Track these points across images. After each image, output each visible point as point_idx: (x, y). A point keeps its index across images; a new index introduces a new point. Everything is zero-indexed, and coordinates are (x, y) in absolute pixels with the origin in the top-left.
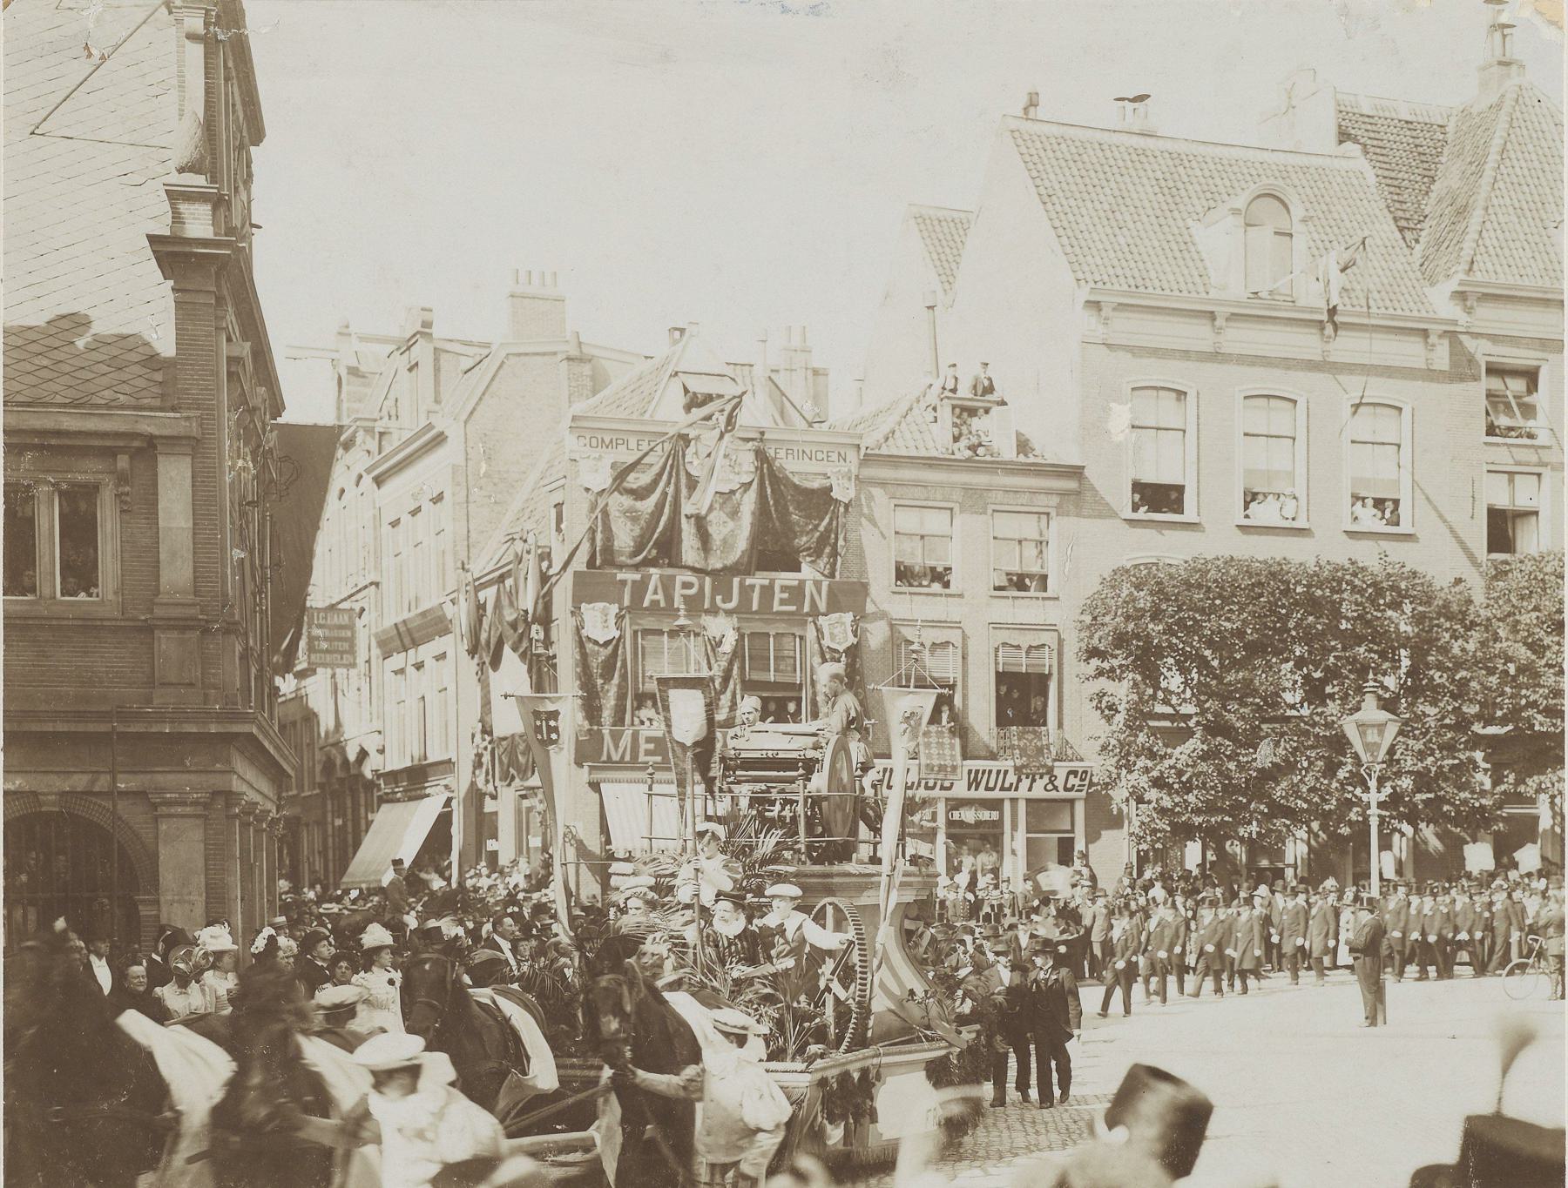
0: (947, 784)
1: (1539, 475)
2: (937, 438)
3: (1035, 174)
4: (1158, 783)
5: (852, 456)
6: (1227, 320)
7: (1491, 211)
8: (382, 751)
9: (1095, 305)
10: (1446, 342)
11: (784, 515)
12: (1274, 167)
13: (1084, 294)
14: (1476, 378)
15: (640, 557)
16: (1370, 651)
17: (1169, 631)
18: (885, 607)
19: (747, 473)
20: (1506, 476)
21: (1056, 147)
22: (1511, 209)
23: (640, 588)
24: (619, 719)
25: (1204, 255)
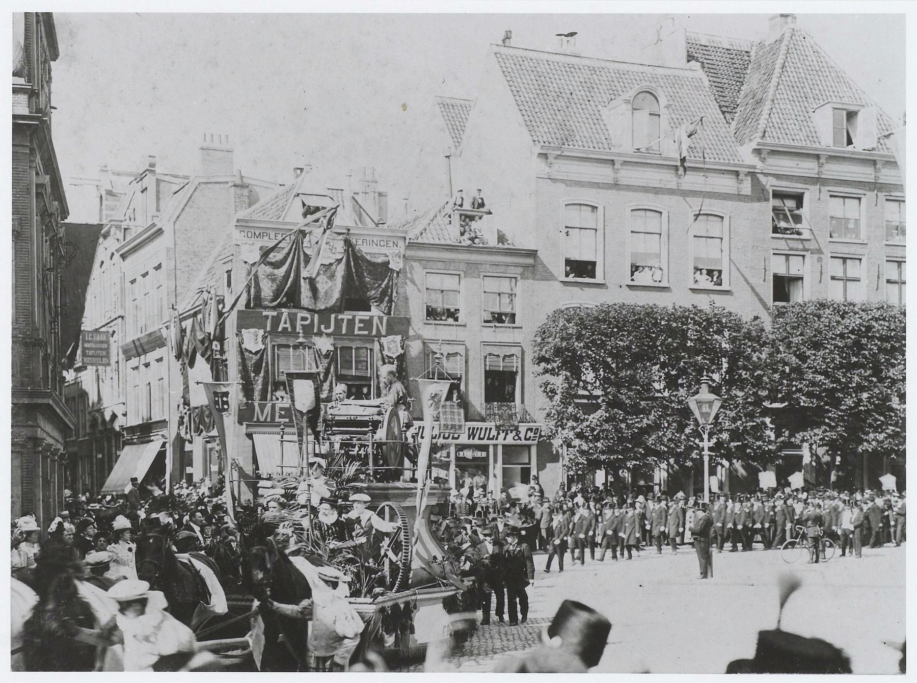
0: (456, 436)
1: (803, 256)
2: (452, 233)
3: (509, 79)
4: (580, 436)
5: (401, 243)
6: (622, 164)
7: (776, 102)
8: (125, 415)
9: (544, 156)
10: (749, 178)
11: (361, 277)
12: (649, 75)
13: (538, 150)
14: (767, 200)
15: (275, 303)
16: (704, 358)
17: (587, 347)
18: (420, 332)
19: (339, 253)
20: (784, 257)
21: (521, 63)
22: (788, 102)
23: (276, 320)
24: (264, 397)
25: (608, 128)
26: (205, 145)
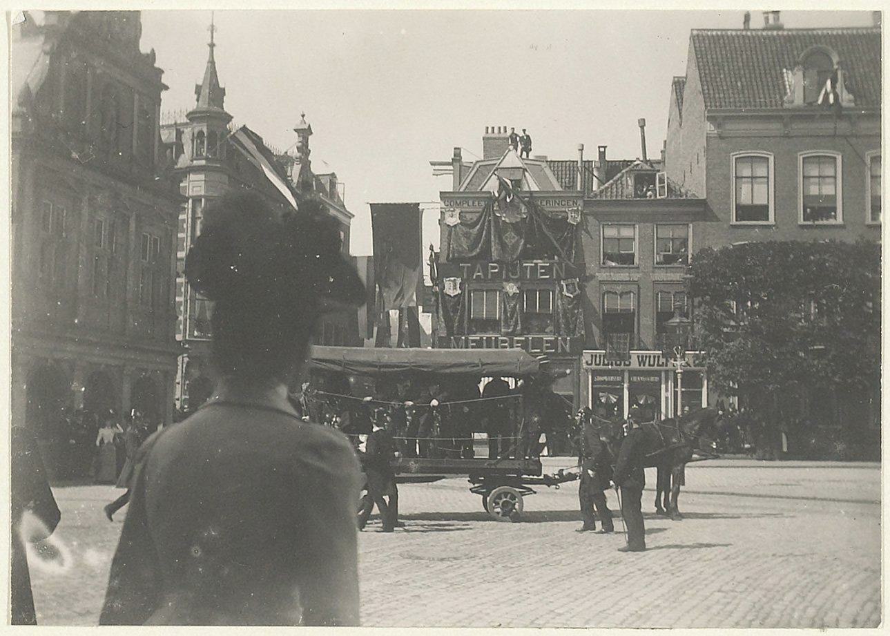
9: (711, 119)
26: (488, 136)
